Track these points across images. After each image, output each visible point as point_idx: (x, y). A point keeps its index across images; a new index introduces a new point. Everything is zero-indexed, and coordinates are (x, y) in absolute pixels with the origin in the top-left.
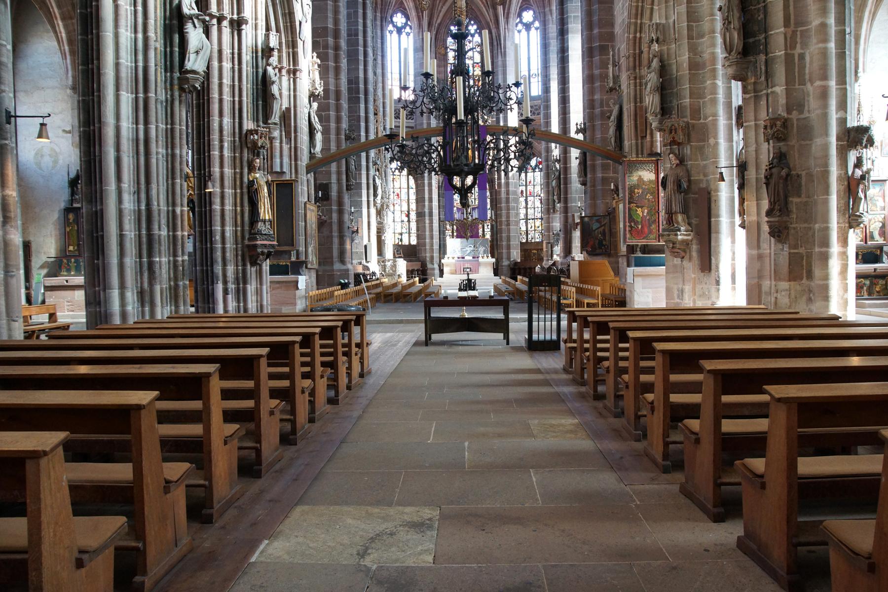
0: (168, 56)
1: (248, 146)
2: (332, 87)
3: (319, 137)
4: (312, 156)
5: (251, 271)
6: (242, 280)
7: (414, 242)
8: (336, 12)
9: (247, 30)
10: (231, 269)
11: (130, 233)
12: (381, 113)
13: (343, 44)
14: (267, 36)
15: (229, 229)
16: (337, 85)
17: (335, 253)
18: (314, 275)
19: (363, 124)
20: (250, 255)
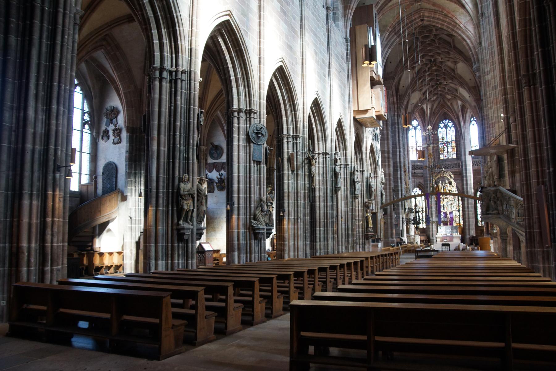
0: (351, 191)
1: (366, 206)
2: (387, 173)
3: (384, 196)
4: (382, 203)
5: (366, 241)
6: (364, 244)
7: (425, 227)
8: (388, 144)
9: (365, 173)
10: (361, 241)
11: (344, 233)
12: (407, 172)
13: (391, 156)
14: (370, 174)
15: (360, 230)
16: (389, 172)
17: (389, 234)
18: (383, 242)
19: (399, 180)
20: (366, 237)
